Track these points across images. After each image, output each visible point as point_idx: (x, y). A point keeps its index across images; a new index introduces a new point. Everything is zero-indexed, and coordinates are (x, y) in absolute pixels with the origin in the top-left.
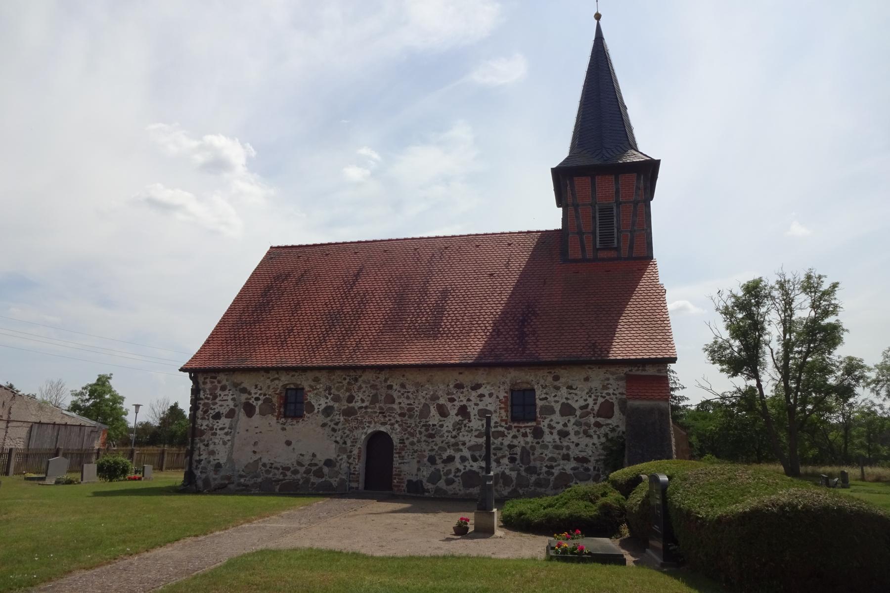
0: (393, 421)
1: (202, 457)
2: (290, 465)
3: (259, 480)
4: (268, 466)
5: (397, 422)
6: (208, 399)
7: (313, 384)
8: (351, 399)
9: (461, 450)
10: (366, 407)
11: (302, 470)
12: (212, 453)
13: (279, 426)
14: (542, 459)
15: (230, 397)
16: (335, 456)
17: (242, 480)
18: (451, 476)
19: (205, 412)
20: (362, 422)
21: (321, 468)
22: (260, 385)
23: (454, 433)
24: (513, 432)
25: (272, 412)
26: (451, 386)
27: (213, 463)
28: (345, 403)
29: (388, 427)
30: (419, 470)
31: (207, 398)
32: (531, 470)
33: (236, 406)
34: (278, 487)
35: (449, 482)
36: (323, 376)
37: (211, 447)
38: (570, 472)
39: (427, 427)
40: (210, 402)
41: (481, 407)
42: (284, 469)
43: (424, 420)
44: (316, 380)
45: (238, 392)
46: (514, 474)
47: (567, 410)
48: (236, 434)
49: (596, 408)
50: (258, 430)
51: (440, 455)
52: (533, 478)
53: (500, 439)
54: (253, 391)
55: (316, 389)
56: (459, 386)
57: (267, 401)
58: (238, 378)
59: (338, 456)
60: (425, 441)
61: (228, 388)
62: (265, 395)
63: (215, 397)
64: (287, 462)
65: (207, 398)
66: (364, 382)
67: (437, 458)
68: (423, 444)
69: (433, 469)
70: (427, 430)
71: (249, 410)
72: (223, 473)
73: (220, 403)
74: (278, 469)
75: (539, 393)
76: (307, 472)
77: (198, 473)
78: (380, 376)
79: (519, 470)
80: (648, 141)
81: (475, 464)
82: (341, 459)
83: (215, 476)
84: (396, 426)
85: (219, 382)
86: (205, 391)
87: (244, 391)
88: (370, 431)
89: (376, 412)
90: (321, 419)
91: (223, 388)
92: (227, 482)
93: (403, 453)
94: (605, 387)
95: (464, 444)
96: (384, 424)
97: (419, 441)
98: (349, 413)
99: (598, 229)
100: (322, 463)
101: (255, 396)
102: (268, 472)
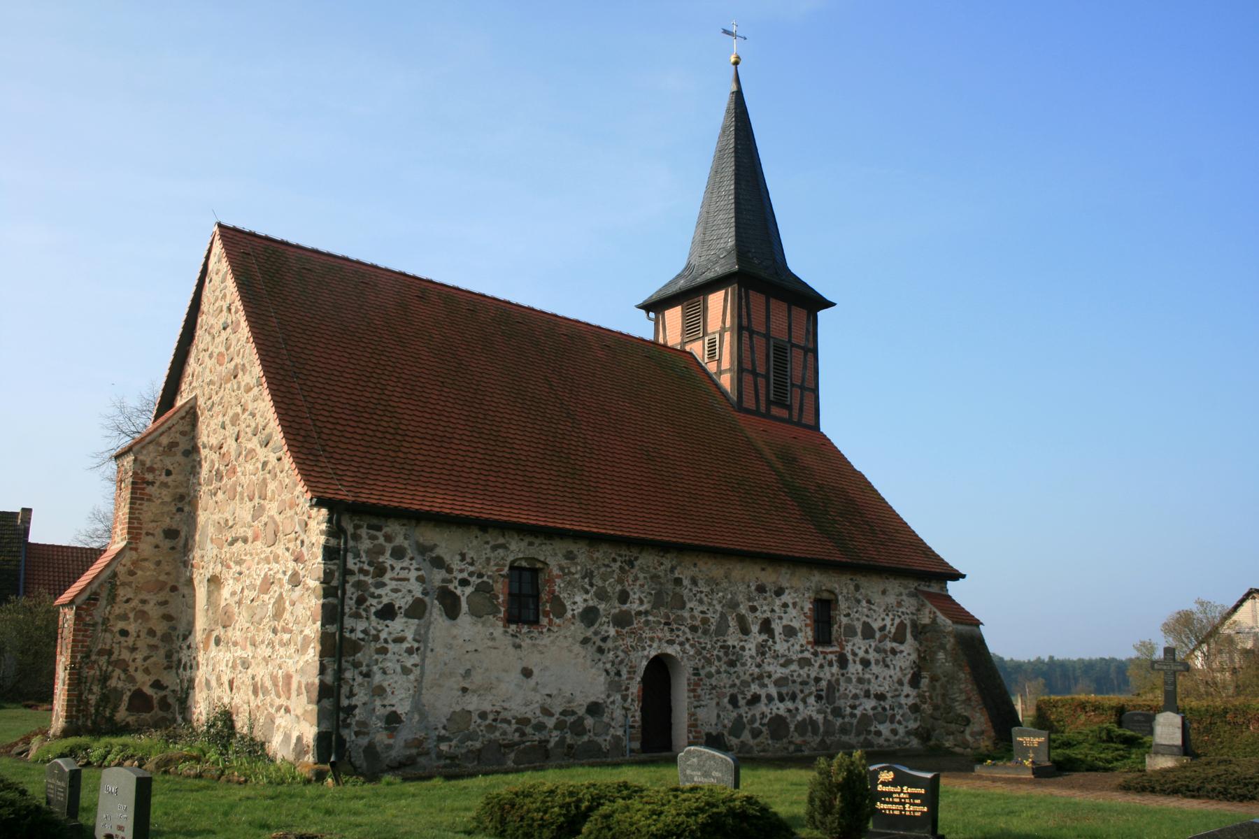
0: (682, 639)
1: (354, 701)
2: (529, 715)
3: (478, 745)
4: (491, 717)
5: (688, 640)
6: (366, 573)
7: (564, 562)
8: (624, 597)
9: (766, 686)
10: (646, 613)
11: (551, 722)
12: (380, 691)
13: (508, 640)
14: (846, 696)
15: (413, 575)
16: (603, 696)
17: (444, 747)
18: (757, 725)
19: (361, 601)
20: (641, 639)
21: (581, 719)
22: (471, 554)
23: (758, 660)
24: (820, 660)
25: (495, 612)
26: (753, 588)
27: (380, 711)
28: (616, 604)
29: (678, 648)
30: (719, 716)
31: (361, 571)
32: (837, 712)
33: (425, 593)
34: (512, 756)
35: (756, 734)
36: (581, 550)
37: (377, 678)
38: (871, 713)
39: (725, 647)
40: (369, 579)
41: (785, 622)
42: (519, 721)
43: (721, 638)
44: (570, 556)
45: (427, 565)
46: (820, 718)
47: (868, 632)
48: (429, 653)
49: (893, 630)
50: (471, 647)
51: (743, 693)
52: (839, 721)
53: (806, 669)
54: (456, 564)
55: (570, 573)
56: (761, 589)
57: (484, 589)
58: (428, 535)
59: (608, 696)
60: (726, 672)
61: (410, 553)
62: (480, 576)
63: (381, 571)
64: (523, 709)
65: (361, 571)
66: (642, 569)
67: (740, 697)
68: (724, 675)
69: (735, 714)
70: (726, 654)
71: (451, 607)
72: (406, 733)
73: (393, 584)
74: (509, 722)
75: (843, 605)
76: (560, 726)
77: (348, 735)
78: (664, 560)
79: (825, 713)
80: (802, 261)
81: (781, 706)
82: (613, 703)
83: (388, 741)
84: (687, 646)
85: (388, 538)
86: (357, 555)
87: (438, 563)
88: (653, 654)
89: (659, 623)
90: (578, 629)
91: (398, 553)
92: (414, 751)
93: (699, 691)
94: (899, 604)
95: (770, 676)
96: (671, 642)
97: (718, 672)
98: (622, 620)
99: (772, 374)
100: (584, 710)
101: (460, 576)
102: (491, 728)
